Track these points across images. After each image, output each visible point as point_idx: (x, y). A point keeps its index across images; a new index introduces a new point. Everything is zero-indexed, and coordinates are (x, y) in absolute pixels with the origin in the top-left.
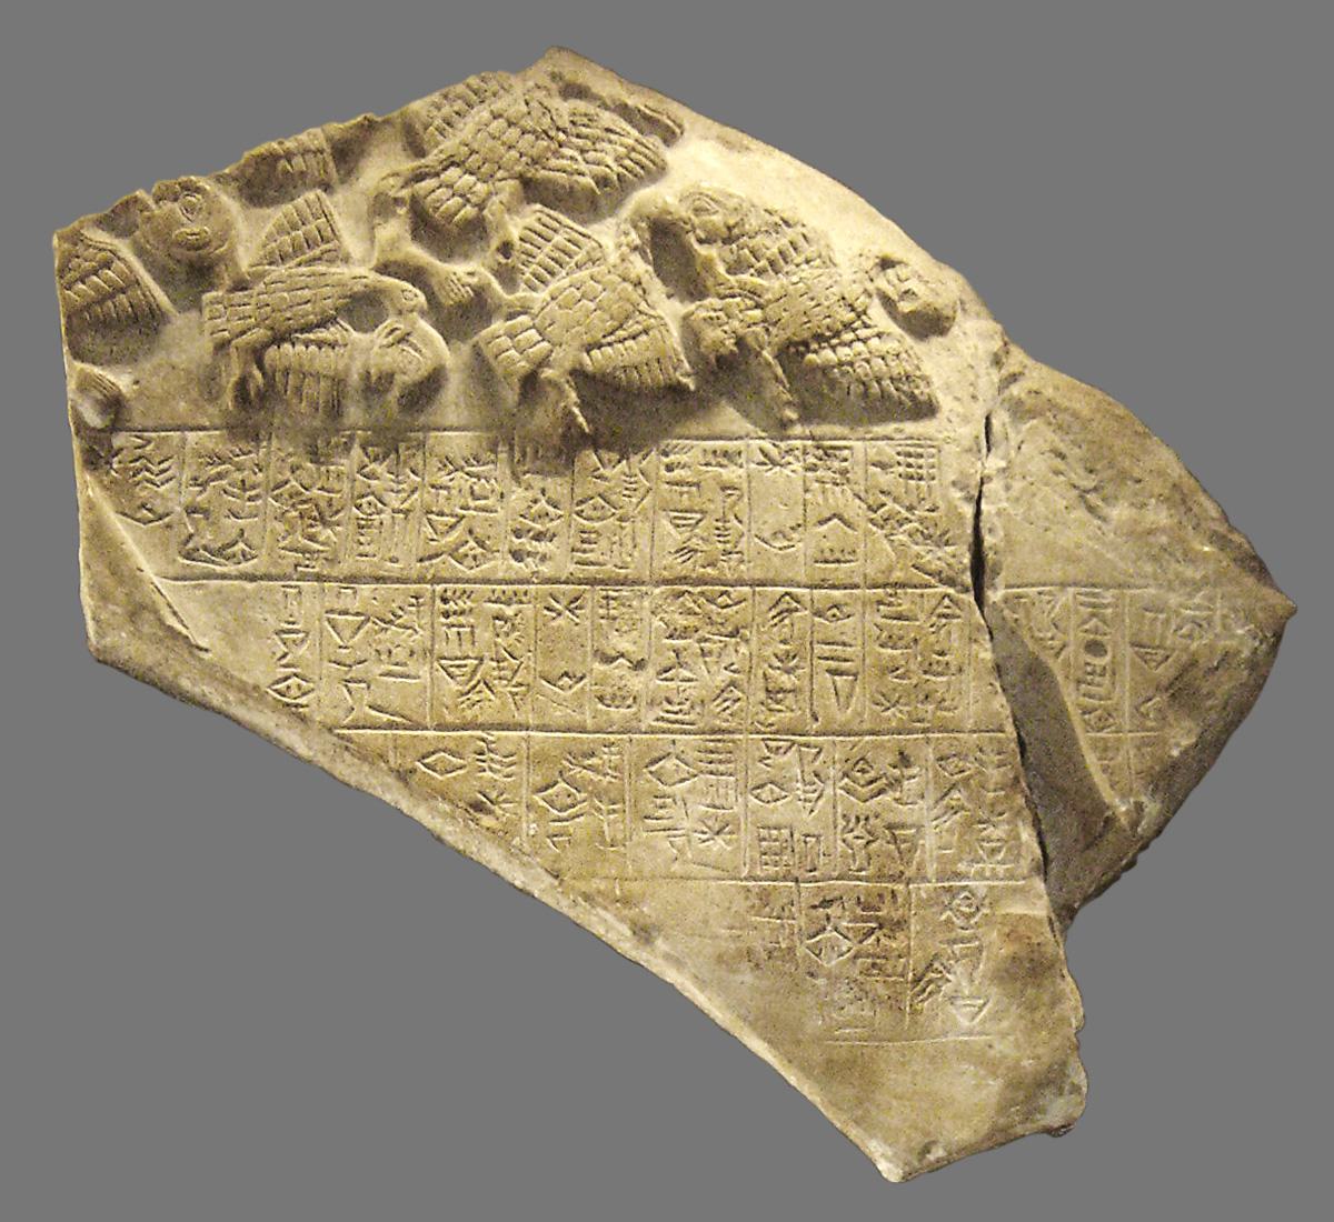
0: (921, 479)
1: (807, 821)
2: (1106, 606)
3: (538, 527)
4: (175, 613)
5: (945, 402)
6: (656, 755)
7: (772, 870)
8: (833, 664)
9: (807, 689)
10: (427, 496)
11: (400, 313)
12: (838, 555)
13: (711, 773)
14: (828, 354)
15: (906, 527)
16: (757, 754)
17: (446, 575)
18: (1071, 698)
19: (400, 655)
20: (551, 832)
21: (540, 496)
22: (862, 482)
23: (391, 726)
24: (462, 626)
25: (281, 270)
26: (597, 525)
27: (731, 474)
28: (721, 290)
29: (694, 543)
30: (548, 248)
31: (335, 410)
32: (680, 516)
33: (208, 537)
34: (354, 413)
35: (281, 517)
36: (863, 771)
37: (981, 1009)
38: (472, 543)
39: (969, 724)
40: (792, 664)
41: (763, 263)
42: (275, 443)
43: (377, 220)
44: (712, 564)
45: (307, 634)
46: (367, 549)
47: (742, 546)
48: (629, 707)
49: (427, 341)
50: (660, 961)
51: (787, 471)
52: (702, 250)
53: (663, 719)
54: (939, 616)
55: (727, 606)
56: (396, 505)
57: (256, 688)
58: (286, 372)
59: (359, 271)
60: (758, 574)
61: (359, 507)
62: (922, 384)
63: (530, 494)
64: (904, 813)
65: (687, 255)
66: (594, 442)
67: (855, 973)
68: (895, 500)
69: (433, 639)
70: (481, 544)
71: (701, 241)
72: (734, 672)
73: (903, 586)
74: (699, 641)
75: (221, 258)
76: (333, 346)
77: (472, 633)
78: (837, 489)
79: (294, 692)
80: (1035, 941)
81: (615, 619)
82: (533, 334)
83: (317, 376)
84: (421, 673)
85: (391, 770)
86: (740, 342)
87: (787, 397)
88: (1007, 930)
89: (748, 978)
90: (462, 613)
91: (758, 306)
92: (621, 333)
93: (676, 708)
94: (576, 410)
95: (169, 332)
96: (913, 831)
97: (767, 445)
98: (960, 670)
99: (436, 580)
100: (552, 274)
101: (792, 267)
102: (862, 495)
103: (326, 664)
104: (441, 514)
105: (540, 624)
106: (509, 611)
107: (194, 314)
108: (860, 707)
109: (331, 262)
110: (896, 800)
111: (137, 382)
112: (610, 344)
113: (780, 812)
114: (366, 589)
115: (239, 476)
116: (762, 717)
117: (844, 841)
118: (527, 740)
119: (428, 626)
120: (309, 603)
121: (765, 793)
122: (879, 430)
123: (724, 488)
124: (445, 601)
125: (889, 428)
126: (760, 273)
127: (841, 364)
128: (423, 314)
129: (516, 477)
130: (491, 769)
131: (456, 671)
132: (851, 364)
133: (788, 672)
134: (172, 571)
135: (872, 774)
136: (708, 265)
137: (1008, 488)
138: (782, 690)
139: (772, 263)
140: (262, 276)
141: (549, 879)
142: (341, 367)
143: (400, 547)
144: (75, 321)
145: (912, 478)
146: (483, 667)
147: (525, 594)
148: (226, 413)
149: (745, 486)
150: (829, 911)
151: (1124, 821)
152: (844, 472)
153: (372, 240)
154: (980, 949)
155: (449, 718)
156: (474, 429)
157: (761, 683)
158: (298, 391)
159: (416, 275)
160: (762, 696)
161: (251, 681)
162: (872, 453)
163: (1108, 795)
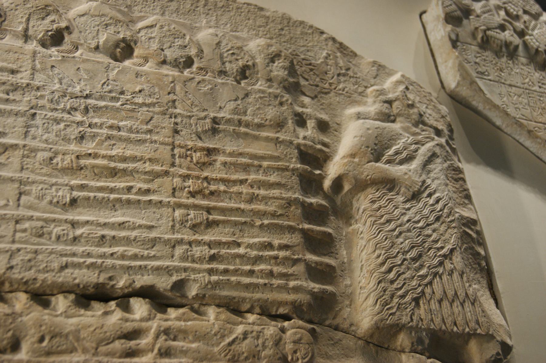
23: (526, 120)
31: (501, 47)
34: (504, 49)
35: (493, 68)
83: (498, 39)
114: (514, 88)
148: (478, 43)
155: (537, 120)
158: (494, 42)
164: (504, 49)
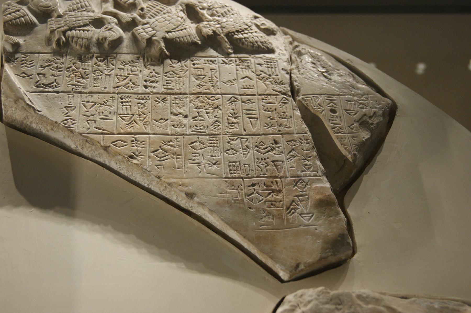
0: (272, 68)
1: (245, 160)
2: (335, 100)
3: (152, 79)
4: (31, 101)
5: (277, 51)
6: (192, 141)
7: (233, 175)
8: (249, 116)
9: (242, 122)
10: (118, 71)
11: (109, 23)
12: (249, 87)
13: (211, 146)
14: (240, 36)
15: (269, 80)
16: (227, 141)
17: (121, 91)
18: (328, 125)
19: (106, 113)
20: (157, 164)
21: (153, 71)
22: (254, 68)
23: (102, 133)
24: (127, 105)
25: (73, 13)
26: (171, 79)
27: (213, 66)
28: (208, 20)
29: (202, 83)
30: (155, 9)
31: (88, 48)
32: (198, 77)
33: (44, 81)
34: (94, 49)
36: (262, 145)
37: (311, 217)
38: (131, 83)
39: (296, 132)
40: (237, 115)
41: (220, 14)
42: (68, 57)
43: (103, 3)
44: (209, 89)
45: (75, 107)
46: (97, 85)
47: (218, 84)
48: (183, 128)
49: (117, 30)
50: (196, 205)
51: (230, 66)
52: (202, 11)
53: (194, 131)
54: (283, 103)
55: (214, 100)
56: (106, 73)
57: (56, 122)
58: (73, 37)
59: (97, 12)
60: (223, 92)
61: (94, 74)
62: (270, 45)
63: (149, 71)
64: (277, 157)
65: (197, 13)
66: (171, 58)
67: (265, 207)
68: (265, 73)
69: (117, 109)
70: (133, 84)
71: (201, 9)
72: (217, 118)
73: (270, 95)
74: (205, 109)
75: (54, 10)
76: (88, 31)
77: (131, 107)
78: (246, 70)
79: (70, 123)
80: (327, 194)
81: (177, 103)
82: (150, 29)
83: (83, 38)
84: (113, 118)
85: (101, 146)
86: (214, 32)
87: (229, 46)
88: (316, 191)
89: (228, 209)
90: (128, 102)
91: (219, 24)
92: (177, 29)
93: (198, 128)
94: (164, 48)
95: (37, 29)
96: (281, 163)
97: (224, 59)
98: (291, 117)
99: (118, 93)
100: (156, 15)
101: (228, 16)
102: (254, 72)
103: (81, 116)
104: (121, 76)
105: (153, 105)
106: (143, 102)
107: (45, 25)
108: (258, 127)
109: (88, 11)
110: (274, 154)
111: (25, 41)
112: (174, 32)
113: (235, 157)
114: (95, 96)
115: (56, 65)
116: (227, 130)
117: (258, 166)
118: (149, 137)
119: (116, 106)
120: (77, 100)
121: (230, 152)
122: (257, 56)
123: (211, 70)
124: (122, 99)
125: (261, 55)
126: (219, 16)
127: (245, 38)
128: (116, 24)
129: (145, 66)
130: (136, 146)
131: (125, 118)
132: (248, 38)
133: (235, 118)
134: (31, 90)
135: (265, 146)
136: (203, 15)
137: (299, 71)
138: (233, 123)
139: (222, 14)
140: (67, 14)
141: (157, 179)
142: (90, 36)
143: (108, 84)
144: (6, 24)
145: (269, 67)
146: (134, 117)
147: (148, 97)
148: (54, 49)
149: (218, 69)
150: (254, 187)
151: (350, 159)
152: (248, 66)
153: (102, 8)
154: (308, 198)
156: (132, 54)
157: (227, 121)
159: (115, 15)
160: (227, 124)
161: (55, 121)
162: (257, 62)
163: (344, 152)
164: (94, 49)
